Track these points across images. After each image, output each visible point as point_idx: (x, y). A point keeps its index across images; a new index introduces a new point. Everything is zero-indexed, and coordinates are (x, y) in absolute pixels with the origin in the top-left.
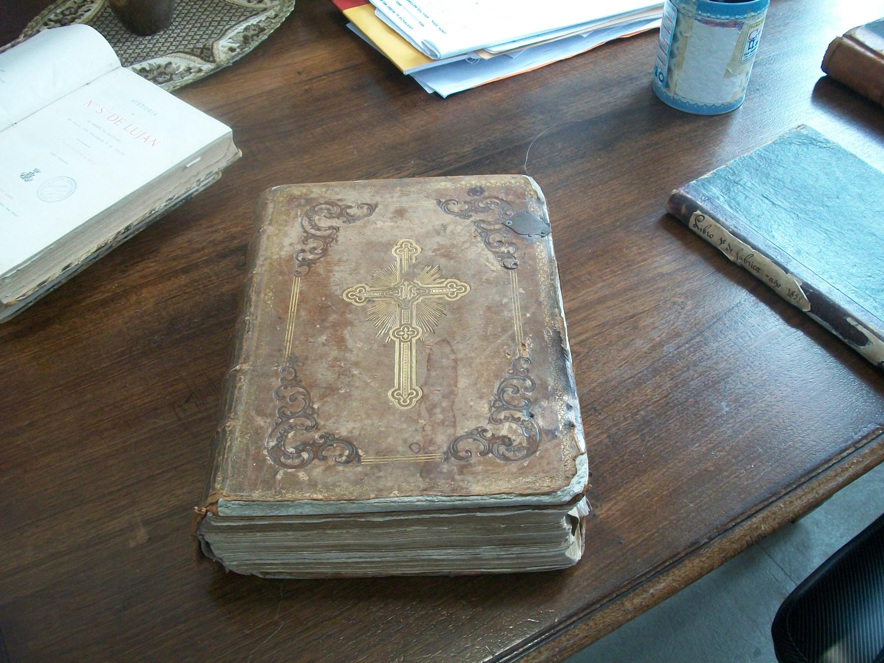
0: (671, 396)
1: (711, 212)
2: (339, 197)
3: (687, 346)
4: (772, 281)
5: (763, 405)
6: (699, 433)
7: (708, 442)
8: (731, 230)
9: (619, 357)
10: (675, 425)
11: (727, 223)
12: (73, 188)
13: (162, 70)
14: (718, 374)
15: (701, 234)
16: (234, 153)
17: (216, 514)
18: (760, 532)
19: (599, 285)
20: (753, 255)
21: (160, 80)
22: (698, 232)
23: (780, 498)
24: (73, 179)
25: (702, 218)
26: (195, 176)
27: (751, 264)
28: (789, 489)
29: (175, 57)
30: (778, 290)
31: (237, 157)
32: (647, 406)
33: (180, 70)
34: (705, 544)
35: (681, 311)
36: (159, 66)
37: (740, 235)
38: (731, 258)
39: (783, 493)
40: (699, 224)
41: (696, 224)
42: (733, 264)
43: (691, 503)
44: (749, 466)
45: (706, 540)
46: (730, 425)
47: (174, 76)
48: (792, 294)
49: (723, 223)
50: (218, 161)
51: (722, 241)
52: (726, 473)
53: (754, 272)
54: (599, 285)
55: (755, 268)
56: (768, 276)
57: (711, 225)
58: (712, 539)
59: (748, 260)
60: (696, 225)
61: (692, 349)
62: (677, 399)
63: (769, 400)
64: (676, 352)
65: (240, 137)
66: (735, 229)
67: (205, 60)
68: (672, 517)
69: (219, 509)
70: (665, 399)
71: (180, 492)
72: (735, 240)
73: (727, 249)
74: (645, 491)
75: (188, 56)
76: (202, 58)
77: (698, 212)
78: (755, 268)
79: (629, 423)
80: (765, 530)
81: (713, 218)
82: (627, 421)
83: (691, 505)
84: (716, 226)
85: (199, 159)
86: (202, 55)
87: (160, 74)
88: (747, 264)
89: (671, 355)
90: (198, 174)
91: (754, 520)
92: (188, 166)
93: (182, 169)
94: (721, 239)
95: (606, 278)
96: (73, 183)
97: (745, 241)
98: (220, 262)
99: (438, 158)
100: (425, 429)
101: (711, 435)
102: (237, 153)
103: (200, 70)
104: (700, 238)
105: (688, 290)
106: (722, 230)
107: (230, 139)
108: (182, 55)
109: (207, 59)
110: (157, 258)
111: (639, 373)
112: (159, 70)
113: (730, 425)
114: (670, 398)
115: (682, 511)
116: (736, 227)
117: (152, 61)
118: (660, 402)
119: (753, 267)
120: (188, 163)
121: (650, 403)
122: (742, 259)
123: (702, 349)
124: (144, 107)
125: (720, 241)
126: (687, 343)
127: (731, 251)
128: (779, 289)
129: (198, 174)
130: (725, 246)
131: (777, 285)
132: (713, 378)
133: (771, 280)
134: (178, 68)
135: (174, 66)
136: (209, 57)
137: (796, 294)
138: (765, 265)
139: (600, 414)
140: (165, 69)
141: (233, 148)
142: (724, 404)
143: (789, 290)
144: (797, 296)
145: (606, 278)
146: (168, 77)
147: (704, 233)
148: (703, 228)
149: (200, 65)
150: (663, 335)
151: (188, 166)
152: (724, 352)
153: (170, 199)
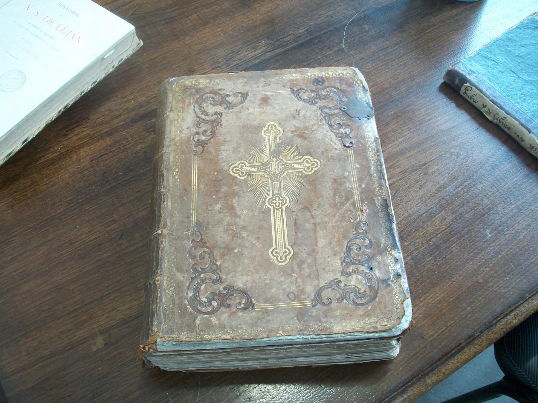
0: (452, 226)
1: (477, 84)
2: (219, 87)
3: (462, 187)
5: (513, 232)
6: (472, 254)
7: (478, 261)
8: (490, 99)
9: (417, 196)
10: (456, 249)
11: (488, 93)
12: (24, 80)
14: (483, 209)
15: (469, 99)
16: (136, 43)
17: (156, 350)
18: (512, 325)
19: (401, 140)
20: (506, 118)
22: (467, 98)
23: (526, 301)
24: (23, 73)
25: (470, 88)
26: (111, 63)
28: (532, 294)
30: (523, 144)
31: (140, 46)
32: (437, 234)
34: (478, 336)
35: (457, 159)
37: (497, 103)
38: (489, 118)
39: (527, 298)
40: (468, 93)
41: (465, 92)
42: (491, 122)
43: (468, 307)
44: (506, 278)
45: (479, 334)
46: (492, 248)
48: (533, 148)
49: (485, 93)
50: (126, 51)
51: (484, 106)
52: (491, 284)
53: (506, 130)
54: (401, 140)
56: (515, 134)
57: (476, 95)
58: (482, 333)
59: (502, 121)
60: (465, 93)
61: (465, 189)
62: (457, 228)
63: (517, 228)
64: (454, 192)
65: (140, 31)
66: (494, 98)
68: (456, 318)
69: (158, 347)
70: (448, 229)
71: (122, 308)
72: (493, 106)
74: (438, 298)
77: (468, 84)
79: (425, 248)
80: (516, 323)
81: (478, 89)
82: (424, 246)
83: (468, 308)
84: (480, 95)
85: (113, 51)
88: (501, 123)
89: (451, 194)
90: (113, 61)
91: (509, 317)
92: (105, 57)
93: (102, 59)
94: (483, 104)
95: (405, 134)
96: (23, 76)
97: (501, 108)
98: (133, 126)
99: (281, 39)
100: (298, 281)
101: (480, 255)
102: (139, 44)
104: (467, 101)
105: (461, 143)
106: (484, 99)
107: (134, 34)
110: (88, 124)
111: (430, 209)
113: (492, 248)
114: (452, 228)
115: (462, 313)
116: (493, 96)
118: (445, 231)
119: (505, 126)
120: (105, 55)
121: (438, 232)
123: (472, 189)
124: (68, 9)
126: (461, 185)
127: (490, 114)
128: (523, 143)
129: (113, 61)
132: (480, 212)
133: (518, 136)
137: (535, 148)
138: (514, 126)
139: (406, 241)
141: (137, 40)
142: (487, 232)
145: (405, 134)
147: (471, 99)
148: (471, 95)
150: (445, 179)
151: (105, 57)
152: (487, 192)
153: (94, 82)
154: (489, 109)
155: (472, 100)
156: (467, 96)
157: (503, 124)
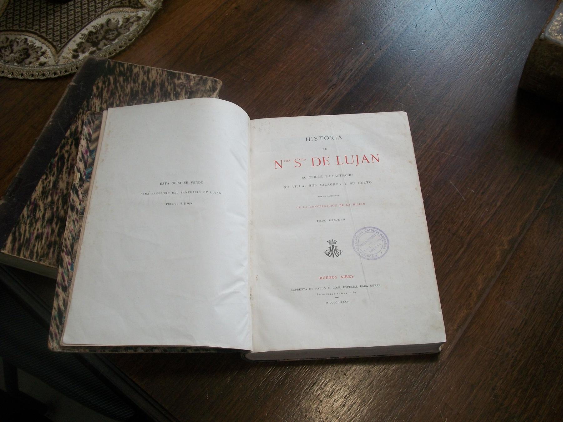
13: (105, 28)
21: (111, 37)
29: (111, 13)
33: (121, 23)
36: (102, 26)
47: (121, 30)
67: (135, 8)
75: (121, 9)
76: (132, 7)
86: (131, 4)
87: (107, 32)
103: (139, 18)
108: (115, 10)
109: (136, 6)
112: (104, 29)
117: (94, 23)
134: (118, 21)
135: (113, 21)
136: (137, 4)
140: (108, 26)
146: (116, 33)
149: (134, 14)
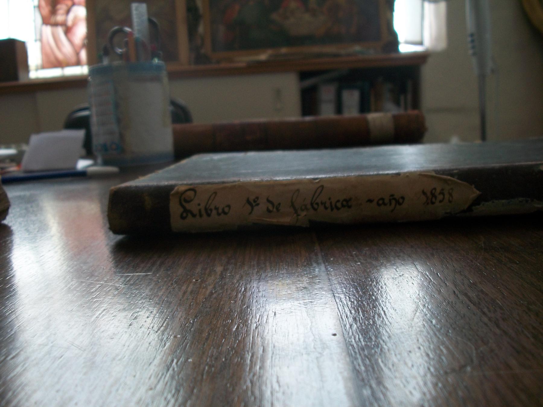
4: (384, 204)
27: (328, 205)
38: (287, 220)
40: (192, 206)
41: (186, 211)
48: (433, 195)
55: (339, 205)
56: (370, 201)
57: (215, 193)
59: (318, 201)
73: (269, 211)
78: (339, 205)
88: (321, 208)
119: (334, 207)
122: (307, 209)
125: (248, 207)
127: (278, 210)
130: (263, 206)
131: (398, 203)
133: (381, 202)
137: (438, 190)
143: (424, 193)
144: (442, 193)
147: (209, 215)
148: (202, 207)
154: (268, 201)
155: (214, 212)
156: (194, 216)
157: (326, 208)
